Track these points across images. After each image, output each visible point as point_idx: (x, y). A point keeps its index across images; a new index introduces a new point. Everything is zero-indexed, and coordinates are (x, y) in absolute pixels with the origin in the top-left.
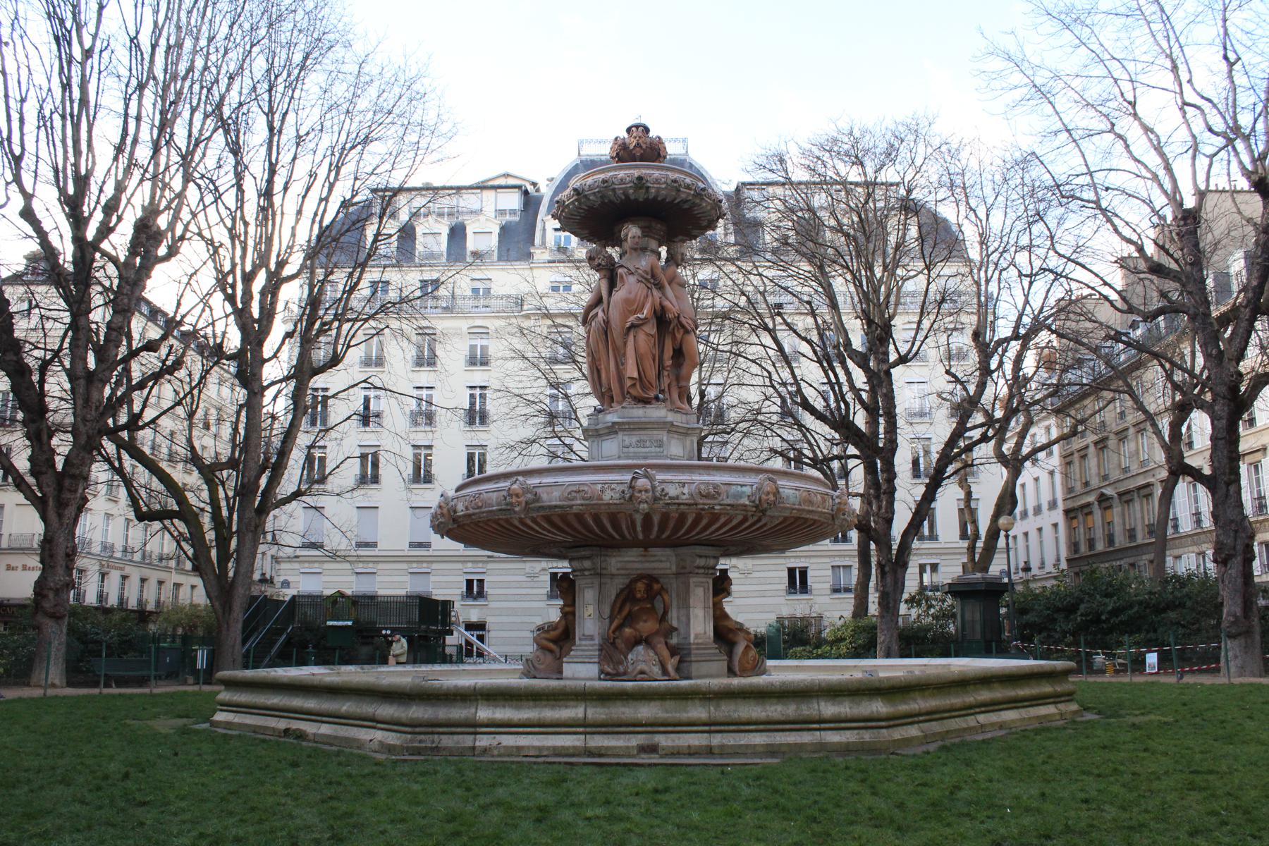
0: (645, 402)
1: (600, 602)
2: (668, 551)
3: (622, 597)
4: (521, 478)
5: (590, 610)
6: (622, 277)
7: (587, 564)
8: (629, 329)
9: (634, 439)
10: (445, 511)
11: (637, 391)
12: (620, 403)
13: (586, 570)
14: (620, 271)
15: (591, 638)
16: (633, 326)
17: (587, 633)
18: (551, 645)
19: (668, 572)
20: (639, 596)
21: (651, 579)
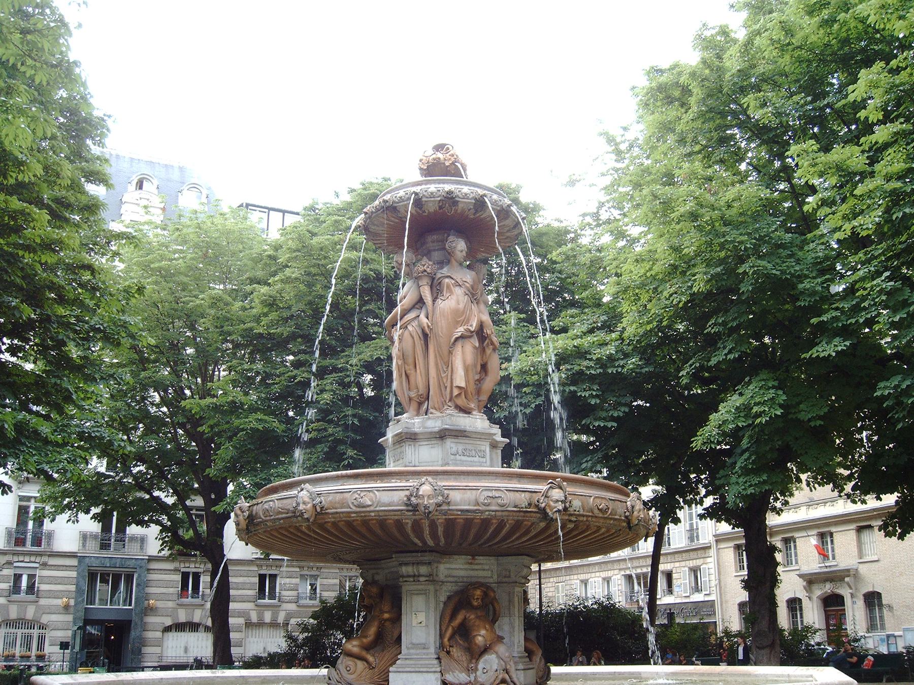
0: (467, 411)
1: (436, 609)
2: (492, 560)
3: (451, 606)
4: (430, 479)
5: (422, 617)
6: (448, 287)
7: (424, 570)
8: (457, 339)
9: (461, 448)
10: (309, 506)
11: (461, 402)
12: (439, 409)
13: (419, 576)
14: (447, 280)
15: (424, 647)
16: (462, 337)
17: (414, 641)
18: (364, 653)
19: (491, 580)
20: (476, 604)
21: (486, 588)
